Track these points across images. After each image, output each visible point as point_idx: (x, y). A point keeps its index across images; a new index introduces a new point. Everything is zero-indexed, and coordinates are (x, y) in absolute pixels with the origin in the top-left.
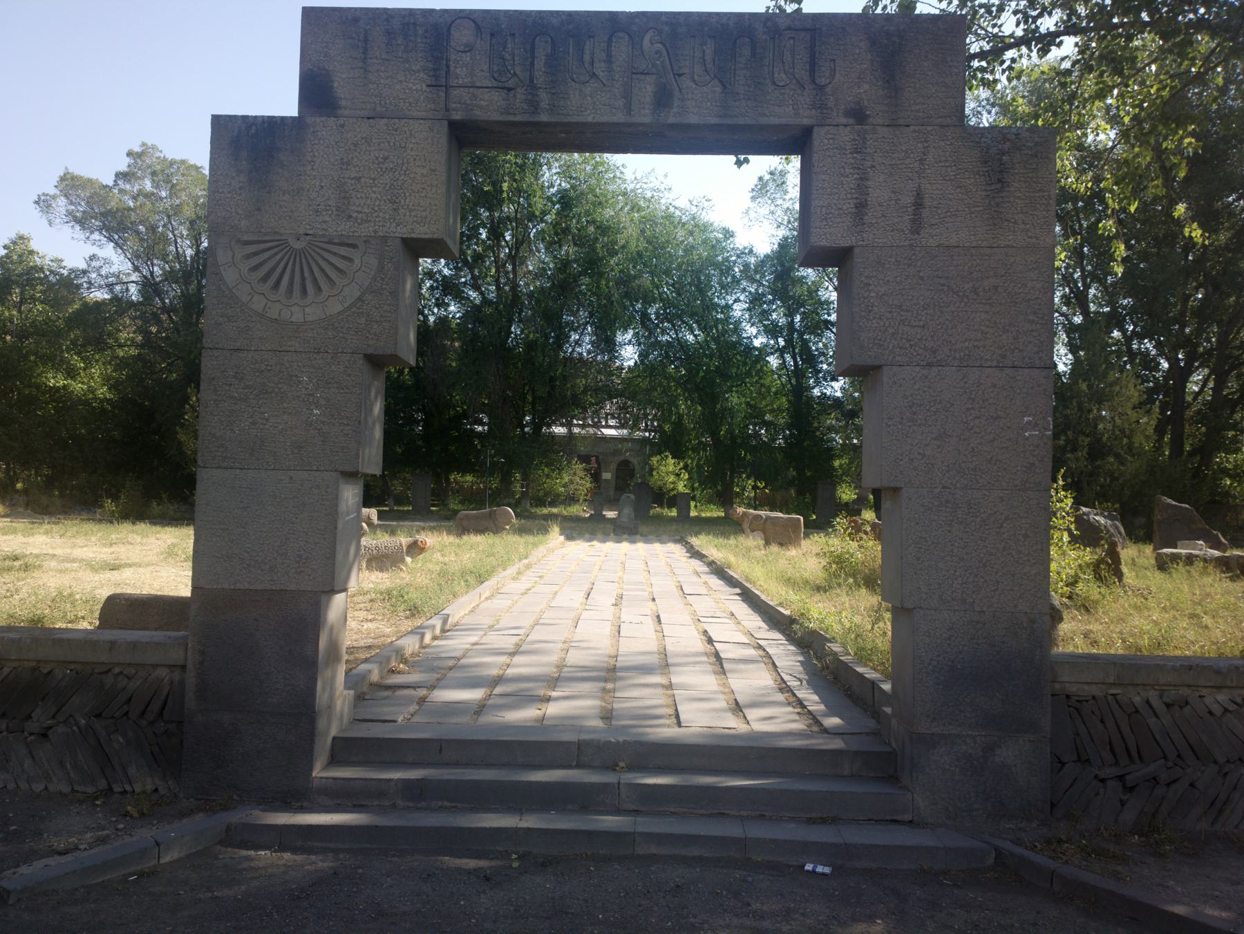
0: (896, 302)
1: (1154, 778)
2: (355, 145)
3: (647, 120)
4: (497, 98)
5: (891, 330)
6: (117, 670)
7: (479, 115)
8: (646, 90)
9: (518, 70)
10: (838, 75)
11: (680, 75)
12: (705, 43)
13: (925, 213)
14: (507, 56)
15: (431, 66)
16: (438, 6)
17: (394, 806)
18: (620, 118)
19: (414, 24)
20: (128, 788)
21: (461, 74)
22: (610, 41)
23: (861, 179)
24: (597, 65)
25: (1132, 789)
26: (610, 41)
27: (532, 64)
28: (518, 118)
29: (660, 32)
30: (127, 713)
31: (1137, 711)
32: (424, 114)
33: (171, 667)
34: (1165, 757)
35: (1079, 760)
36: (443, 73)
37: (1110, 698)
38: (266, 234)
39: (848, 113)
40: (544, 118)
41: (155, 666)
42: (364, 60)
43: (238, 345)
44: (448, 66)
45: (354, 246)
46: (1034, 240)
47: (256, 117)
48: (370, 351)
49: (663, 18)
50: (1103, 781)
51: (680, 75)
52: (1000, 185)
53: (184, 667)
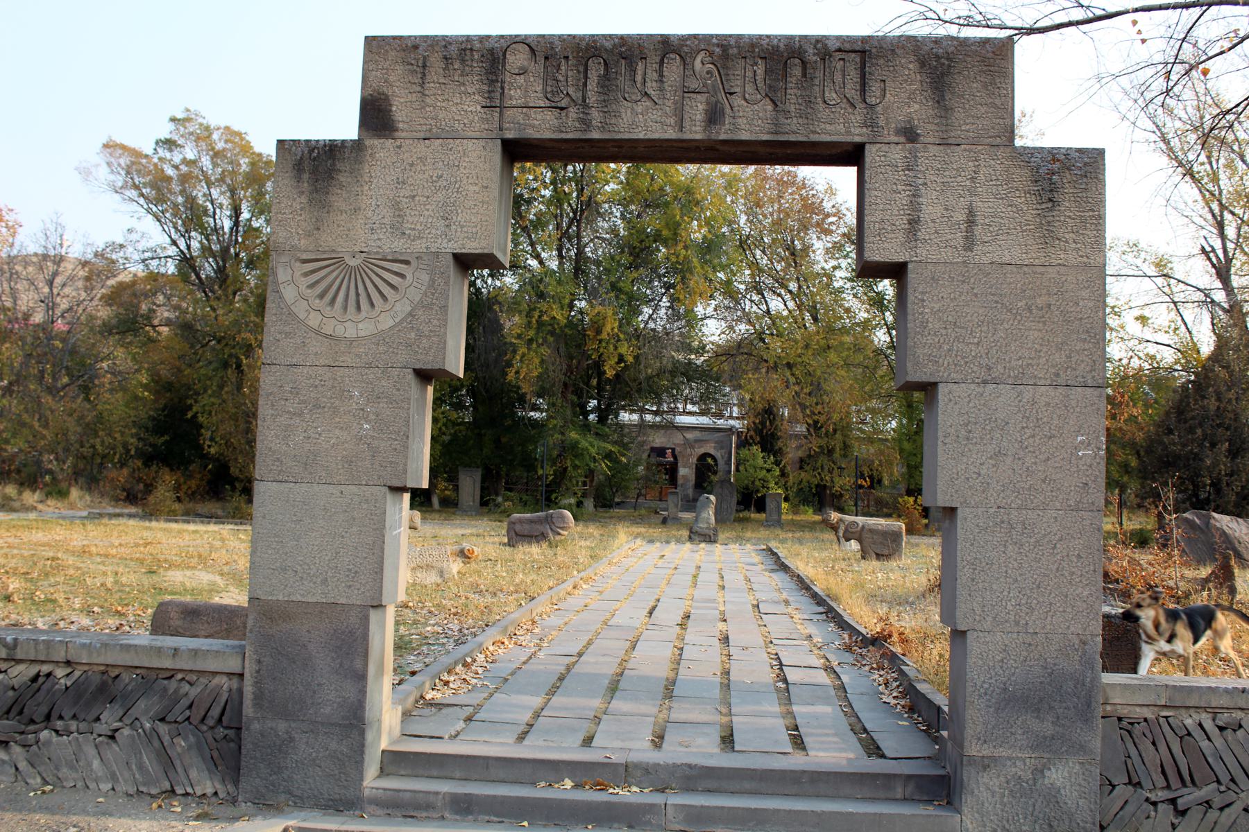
0: (950, 318)
1: (1207, 802)
2: (412, 165)
3: (698, 137)
4: (550, 117)
5: (946, 347)
6: (180, 676)
8: (697, 109)
10: (888, 95)
11: (731, 94)
12: (756, 64)
13: (978, 230)
14: (560, 78)
16: (494, 32)
17: (443, 818)
18: (671, 134)
19: (471, 50)
20: (190, 790)
21: (515, 95)
22: (662, 63)
23: (914, 196)
24: (649, 84)
25: (1183, 813)
26: (662, 63)
27: (585, 85)
29: (711, 54)
30: (188, 719)
31: (1189, 734)
32: (478, 134)
33: (229, 674)
34: (1219, 782)
35: (1130, 783)
36: (498, 95)
37: (1161, 720)
38: (324, 252)
39: (898, 132)
40: (595, 135)
41: (215, 673)
42: (422, 85)
43: (294, 361)
44: (503, 88)
45: (407, 263)
46: (1085, 259)
47: (318, 141)
48: (417, 367)
49: (714, 41)
50: (1154, 804)
51: (731, 94)
52: (1050, 205)
53: (241, 675)
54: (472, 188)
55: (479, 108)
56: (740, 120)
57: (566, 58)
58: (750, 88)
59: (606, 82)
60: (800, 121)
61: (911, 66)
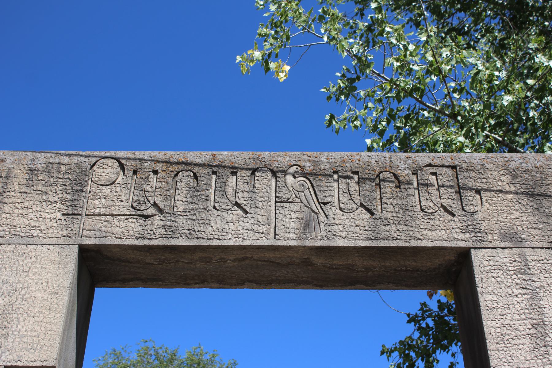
3: (293, 243)
7: (111, 241)
9: (158, 200)
10: (485, 204)
11: (325, 204)
15: (69, 197)
21: (97, 204)
24: (240, 195)
28: (155, 242)
39: (503, 236)
51: (325, 204)
54: (39, 294)
55: (59, 215)
56: (336, 228)
57: (155, 172)
58: (345, 198)
59: (196, 193)
60: (399, 227)
61: (503, 178)
